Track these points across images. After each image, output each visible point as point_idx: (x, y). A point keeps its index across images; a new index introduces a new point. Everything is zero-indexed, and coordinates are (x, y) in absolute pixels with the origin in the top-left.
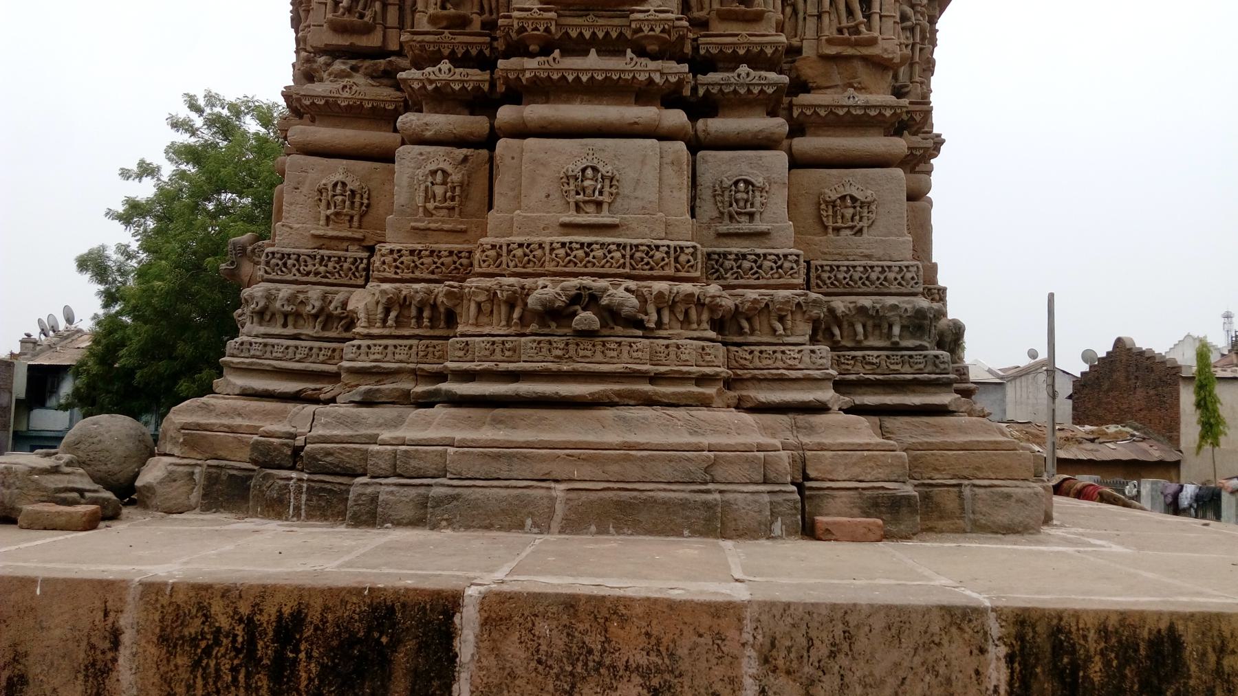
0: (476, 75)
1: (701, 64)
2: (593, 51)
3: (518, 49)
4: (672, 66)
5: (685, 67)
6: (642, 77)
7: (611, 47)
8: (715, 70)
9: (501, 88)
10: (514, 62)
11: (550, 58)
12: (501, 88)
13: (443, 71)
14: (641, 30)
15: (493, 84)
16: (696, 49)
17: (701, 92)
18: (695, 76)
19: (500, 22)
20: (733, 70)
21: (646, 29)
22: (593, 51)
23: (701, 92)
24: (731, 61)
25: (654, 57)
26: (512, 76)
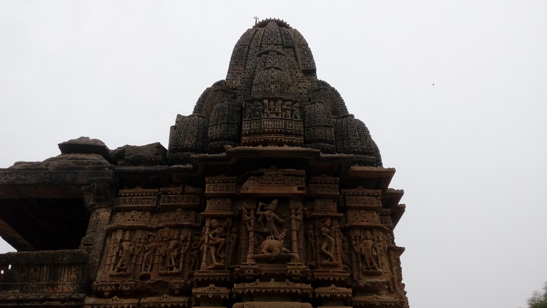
0: (223, 291)
1: (317, 284)
2: (273, 280)
3: (241, 280)
4: (304, 286)
5: (309, 286)
6: (294, 291)
7: (281, 278)
8: (321, 286)
9: (234, 296)
10: (241, 286)
11: (255, 283)
12: (234, 296)
13: (209, 290)
14: (291, 272)
15: (231, 294)
16: (313, 276)
17: (317, 296)
18: (314, 288)
19: (236, 269)
20: (329, 286)
21: (293, 272)
22: (273, 280)
23: (317, 296)
24: (327, 283)
25: (297, 282)
26: (240, 292)
